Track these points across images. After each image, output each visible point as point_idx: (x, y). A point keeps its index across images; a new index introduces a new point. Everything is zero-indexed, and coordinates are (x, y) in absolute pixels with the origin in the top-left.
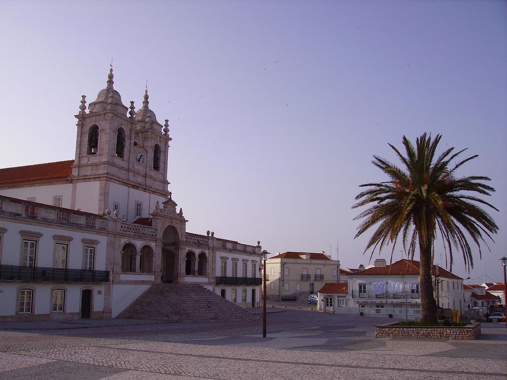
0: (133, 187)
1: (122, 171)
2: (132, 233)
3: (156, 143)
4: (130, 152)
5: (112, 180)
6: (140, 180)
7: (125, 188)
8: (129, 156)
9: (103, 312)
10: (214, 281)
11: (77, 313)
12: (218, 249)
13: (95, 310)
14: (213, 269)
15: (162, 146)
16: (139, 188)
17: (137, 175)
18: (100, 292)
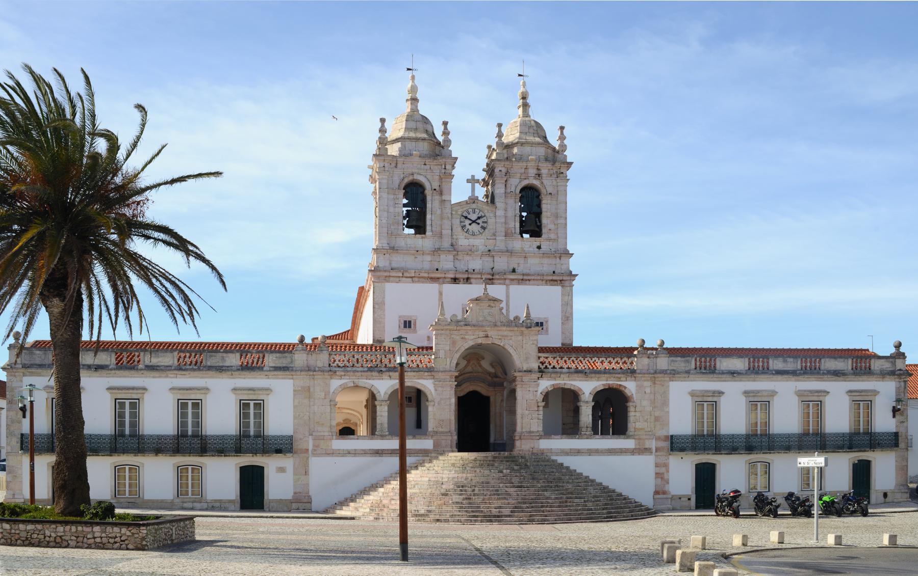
0: (455, 280)
1: (420, 258)
2: (361, 369)
3: (525, 183)
4: (442, 218)
5: (392, 279)
6: (476, 264)
7: (435, 287)
8: (441, 226)
9: (291, 502)
10: (667, 444)
11: (230, 501)
12: (673, 374)
13: (270, 498)
14: (661, 420)
15: (547, 185)
16: (472, 280)
17: (468, 258)
18: (281, 470)
